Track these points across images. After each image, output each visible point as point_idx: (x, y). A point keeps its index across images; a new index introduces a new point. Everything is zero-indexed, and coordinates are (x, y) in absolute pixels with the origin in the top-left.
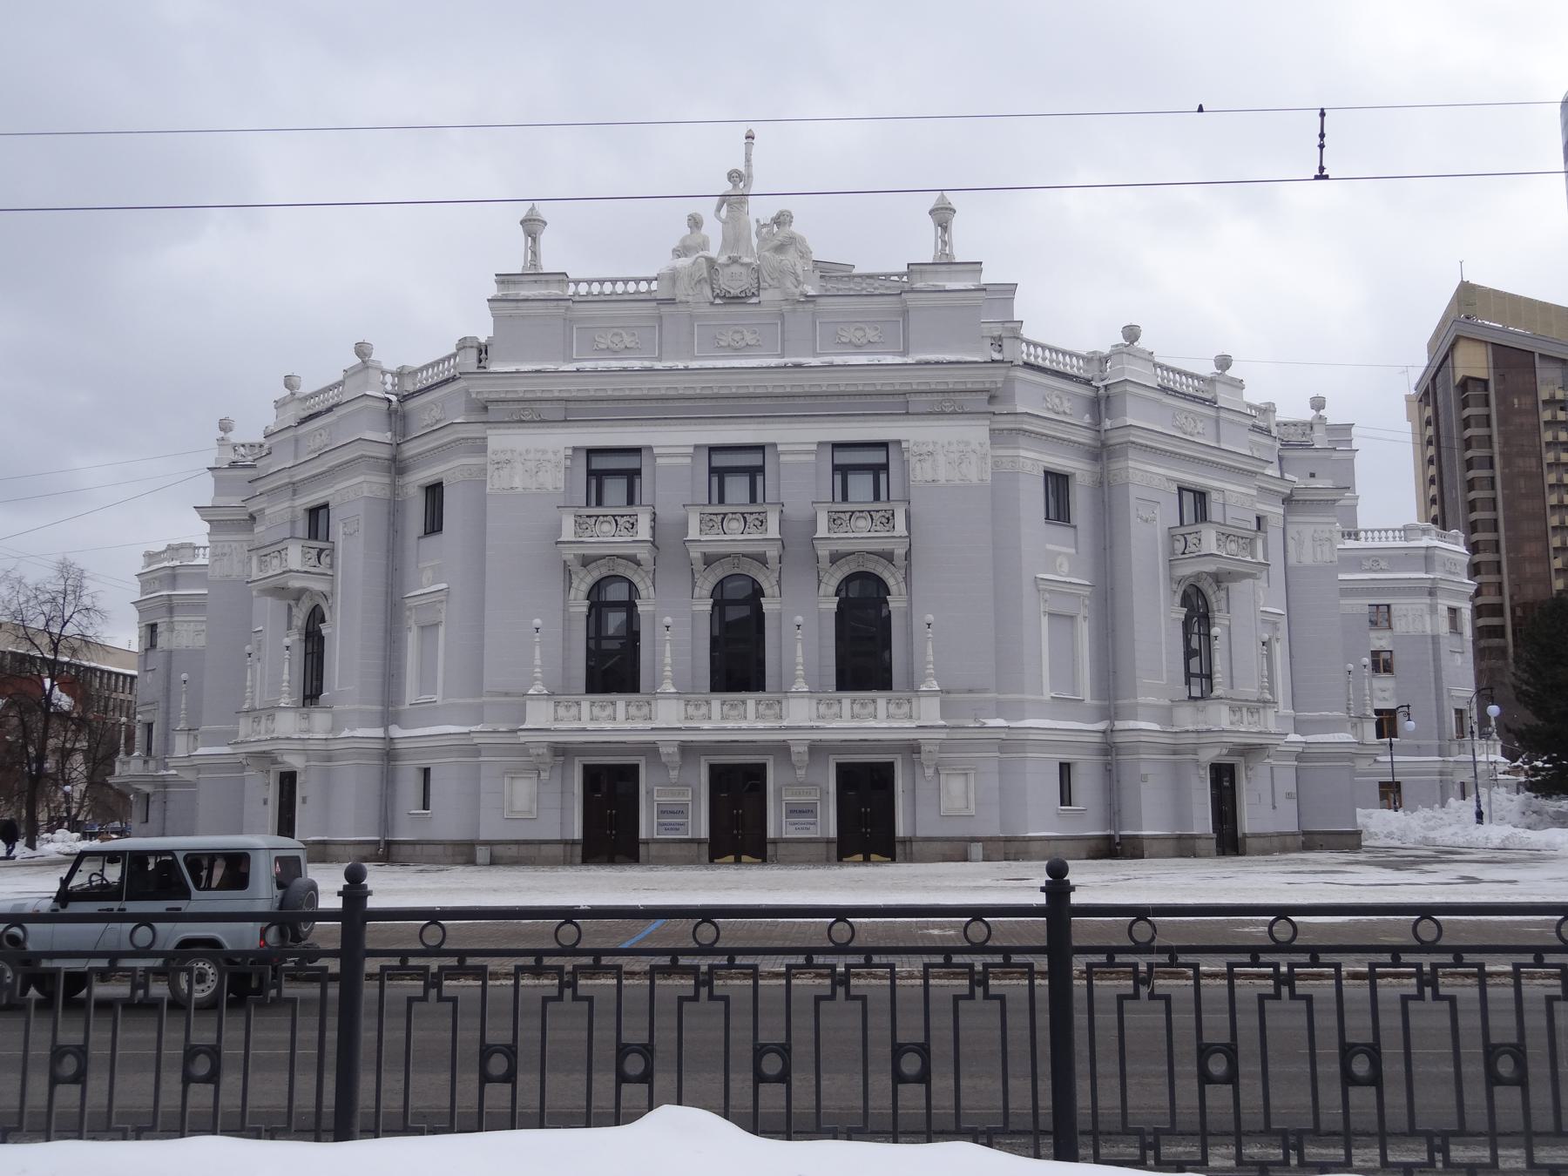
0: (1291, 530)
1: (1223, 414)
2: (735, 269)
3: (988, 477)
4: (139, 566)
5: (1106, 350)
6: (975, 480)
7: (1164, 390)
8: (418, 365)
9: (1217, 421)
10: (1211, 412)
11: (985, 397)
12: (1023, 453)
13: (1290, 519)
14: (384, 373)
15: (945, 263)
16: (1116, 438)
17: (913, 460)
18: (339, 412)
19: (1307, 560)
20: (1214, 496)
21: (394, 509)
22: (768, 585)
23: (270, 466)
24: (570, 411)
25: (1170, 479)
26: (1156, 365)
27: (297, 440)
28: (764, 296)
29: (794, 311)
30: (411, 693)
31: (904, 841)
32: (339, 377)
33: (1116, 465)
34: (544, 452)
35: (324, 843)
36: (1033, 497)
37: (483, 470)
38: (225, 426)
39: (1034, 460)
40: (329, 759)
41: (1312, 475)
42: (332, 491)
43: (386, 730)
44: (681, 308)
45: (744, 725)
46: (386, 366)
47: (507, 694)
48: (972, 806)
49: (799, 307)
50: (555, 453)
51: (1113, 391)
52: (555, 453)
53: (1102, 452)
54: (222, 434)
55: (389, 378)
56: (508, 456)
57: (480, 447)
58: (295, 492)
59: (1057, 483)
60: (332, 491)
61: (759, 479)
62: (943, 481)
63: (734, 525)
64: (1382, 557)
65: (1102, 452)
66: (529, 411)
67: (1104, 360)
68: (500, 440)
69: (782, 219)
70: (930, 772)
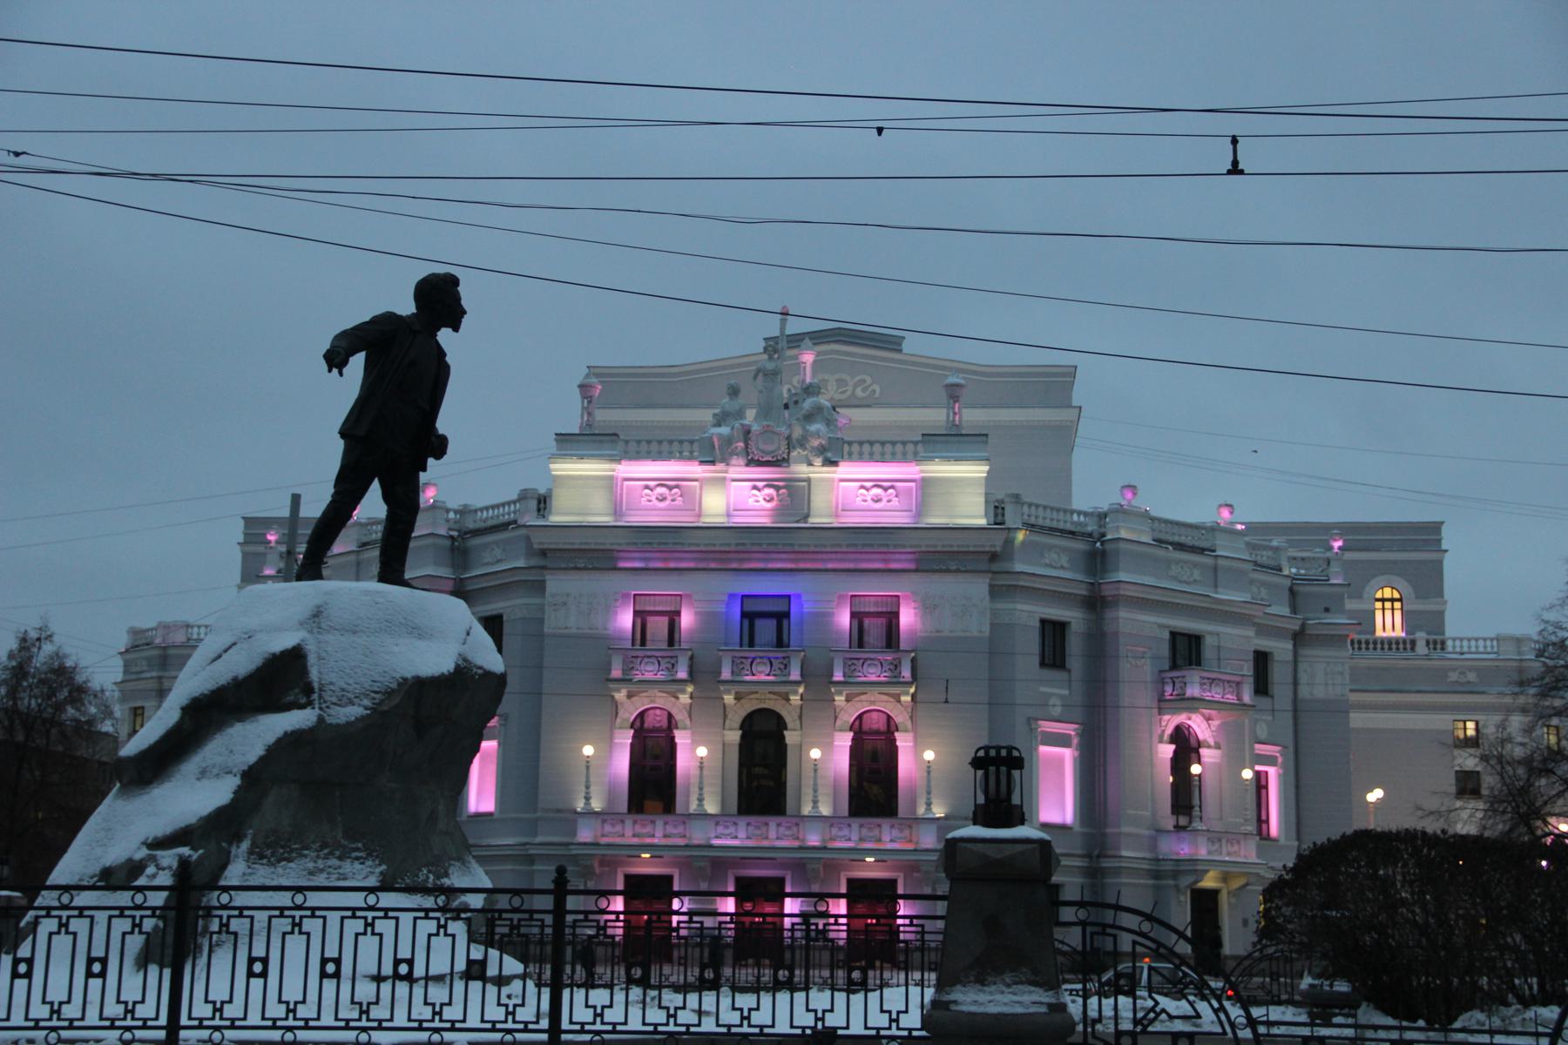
0: (1302, 667)
1: (1221, 562)
3: (987, 629)
4: (123, 642)
5: (1105, 507)
6: (975, 634)
7: (1160, 542)
8: (479, 505)
9: (1215, 569)
10: (1210, 561)
11: (986, 557)
12: (1019, 606)
13: (1303, 652)
14: (448, 511)
16: (1107, 591)
19: (1319, 693)
20: (1209, 641)
22: (790, 718)
25: (1161, 626)
26: (1153, 519)
27: (358, 564)
33: (1109, 614)
36: (1029, 645)
37: (541, 608)
39: (1029, 613)
41: (1327, 610)
45: (765, 843)
46: (449, 505)
51: (1108, 547)
53: (1096, 603)
55: (452, 515)
59: (1054, 632)
61: (785, 622)
62: (946, 633)
63: (761, 668)
64: (1470, 669)
65: (1096, 603)
67: (1102, 516)
68: (556, 584)
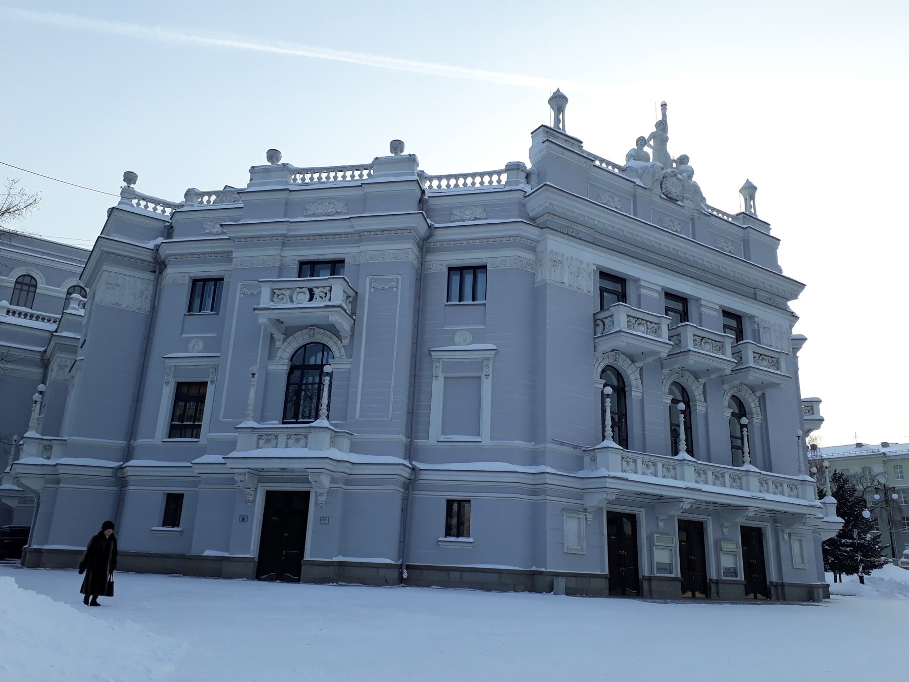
2: (674, 179)
15: (748, 216)
17: (761, 330)
18: (368, 189)
21: (421, 279)
23: (241, 218)
24: (596, 239)
28: (687, 203)
29: (700, 218)
30: (434, 432)
31: (776, 585)
32: (369, 161)
34: (581, 262)
35: (341, 564)
38: (130, 177)
40: (347, 483)
42: (356, 250)
43: (411, 463)
44: (647, 193)
47: (562, 444)
48: (806, 561)
49: (702, 216)
50: (588, 265)
52: (588, 265)
54: (125, 184)
56: (560, 258)
57: (532, 247)
58: (283, 245)
60: (356, 250)
66: (572, 230)
68: (555, 244)
69: (683, 160)
70: (786, 536)
